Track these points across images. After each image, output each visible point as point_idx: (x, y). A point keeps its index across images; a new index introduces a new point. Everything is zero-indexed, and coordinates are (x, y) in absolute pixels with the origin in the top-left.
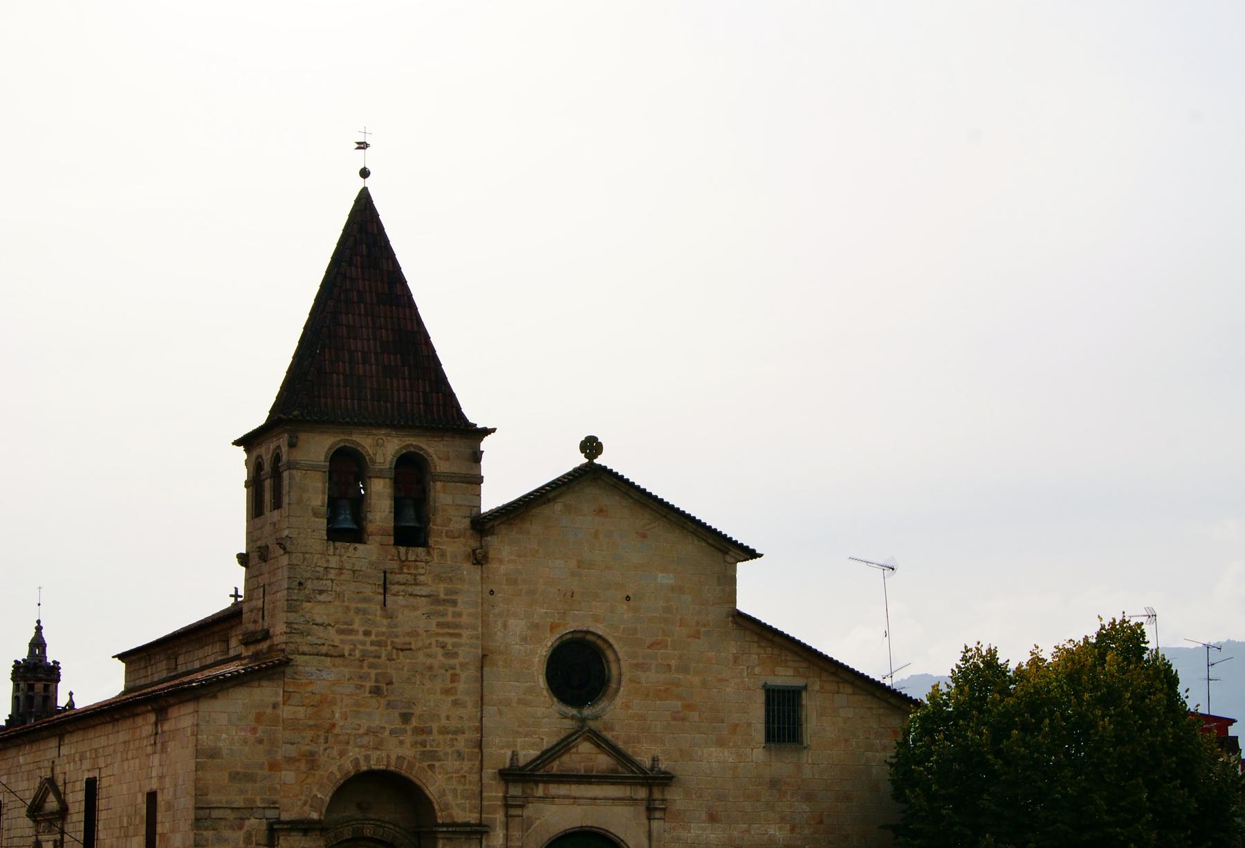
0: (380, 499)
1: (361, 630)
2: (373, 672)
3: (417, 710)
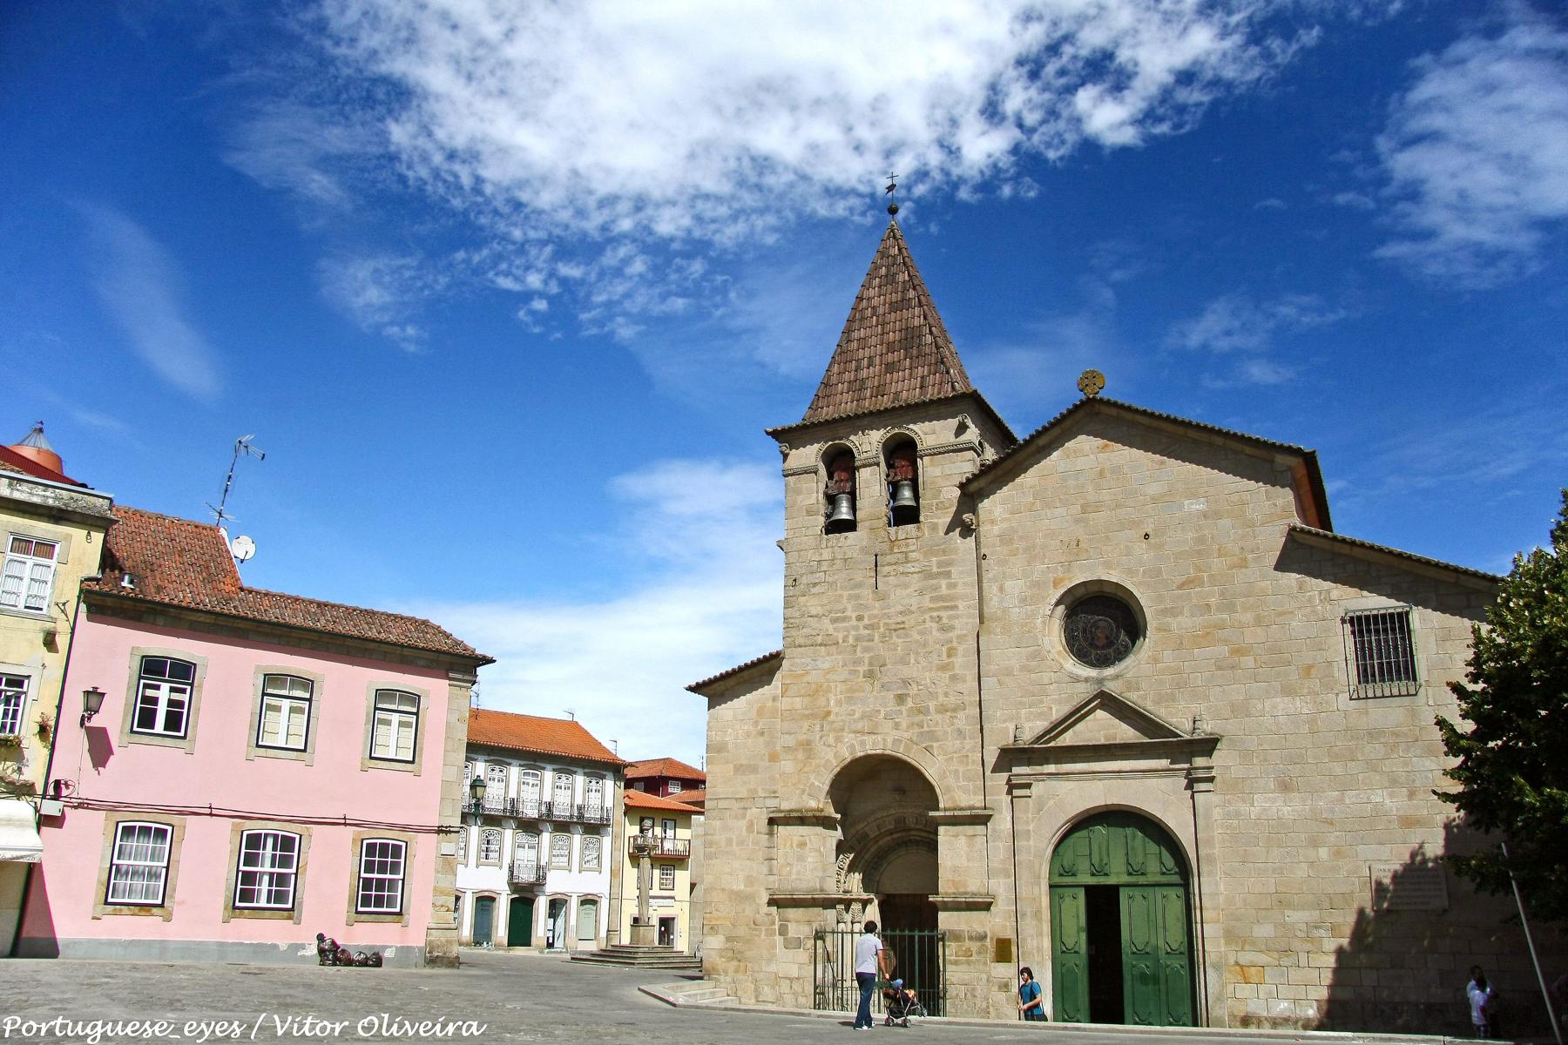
0: (872, 484)
1: (854, 616)
2: (867, 655)
3: (914, 689)
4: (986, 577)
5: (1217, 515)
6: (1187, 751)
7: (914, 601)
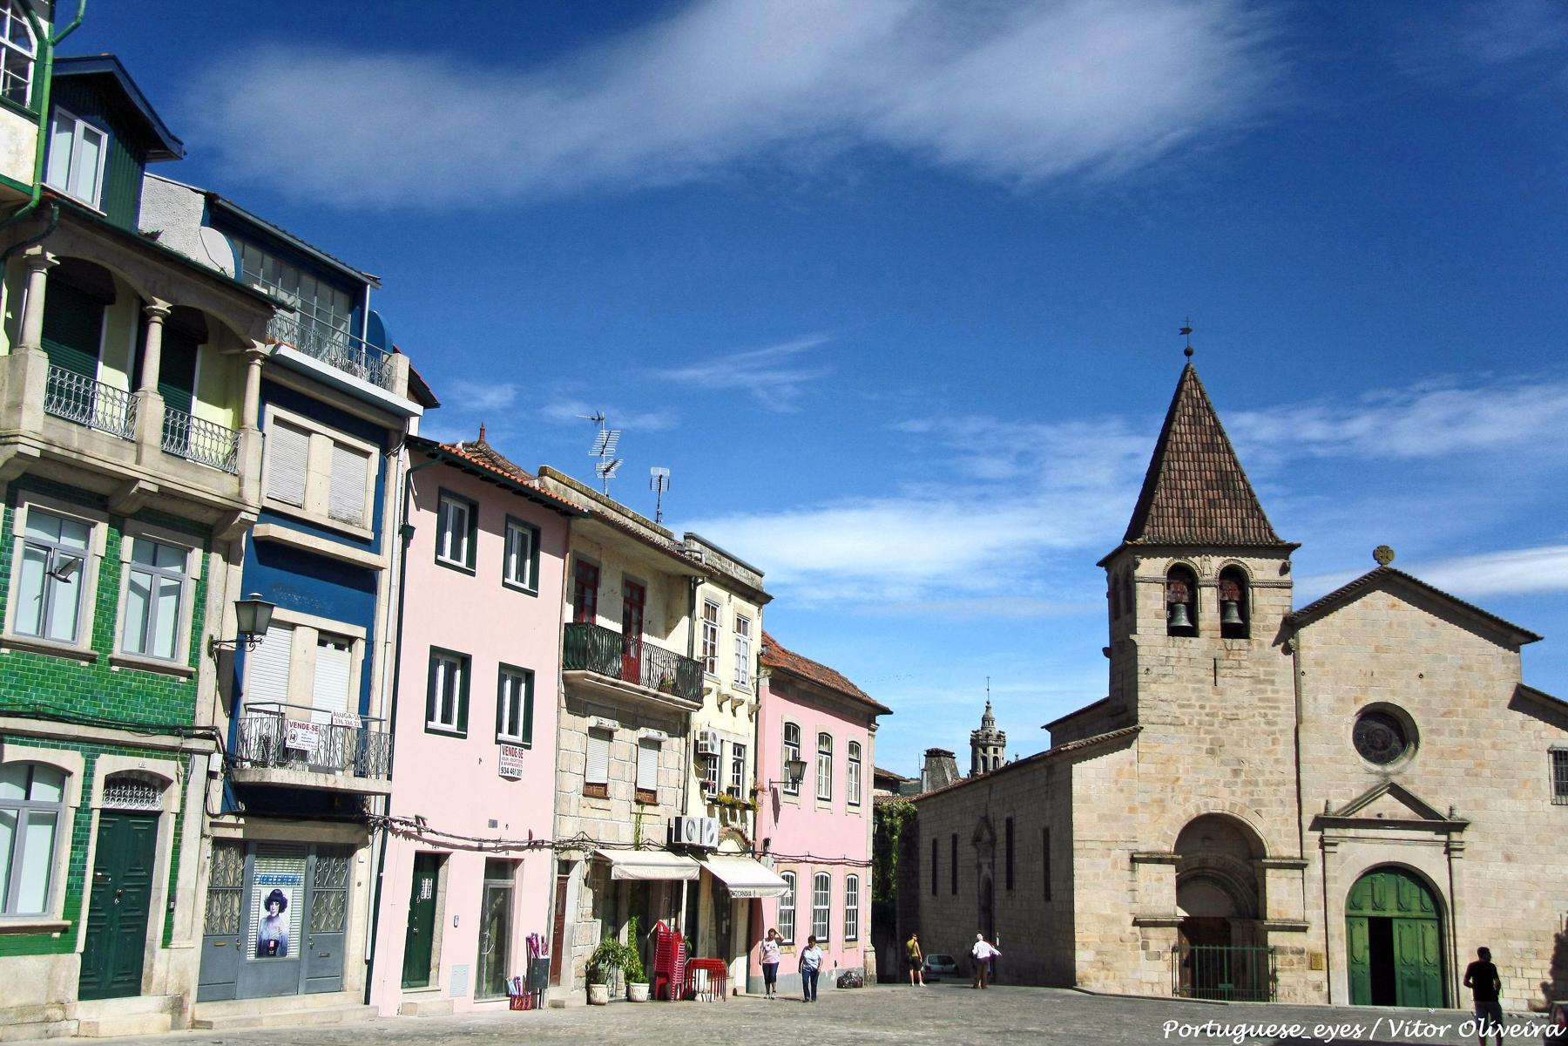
2: (1208, 737)
3: (1246, 767)
4: (1305, 689)
5: (1470, 669)
6: (1447, 827)
7: (1246, 700)
